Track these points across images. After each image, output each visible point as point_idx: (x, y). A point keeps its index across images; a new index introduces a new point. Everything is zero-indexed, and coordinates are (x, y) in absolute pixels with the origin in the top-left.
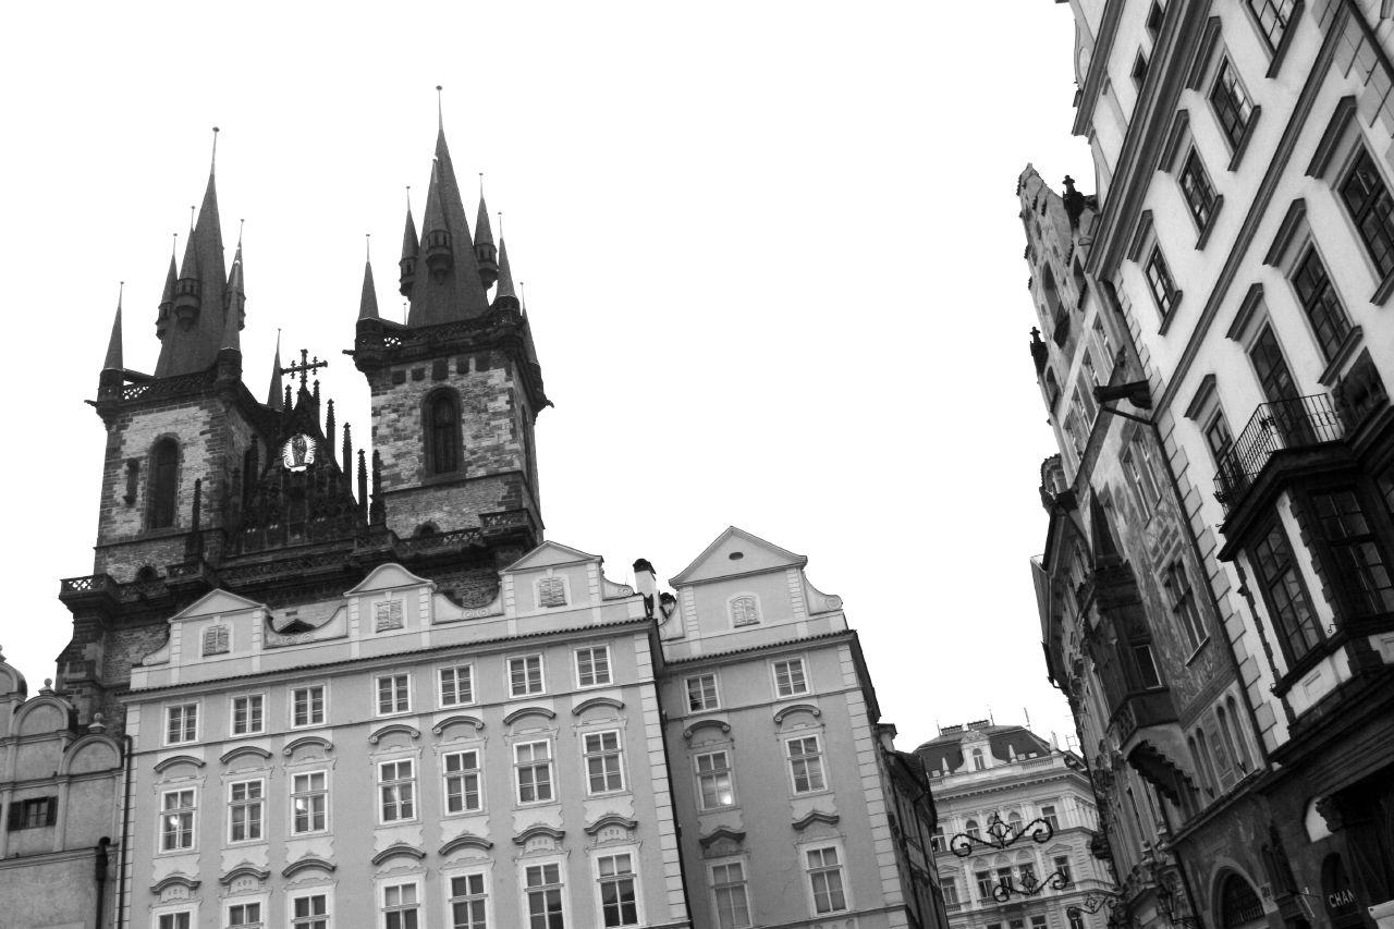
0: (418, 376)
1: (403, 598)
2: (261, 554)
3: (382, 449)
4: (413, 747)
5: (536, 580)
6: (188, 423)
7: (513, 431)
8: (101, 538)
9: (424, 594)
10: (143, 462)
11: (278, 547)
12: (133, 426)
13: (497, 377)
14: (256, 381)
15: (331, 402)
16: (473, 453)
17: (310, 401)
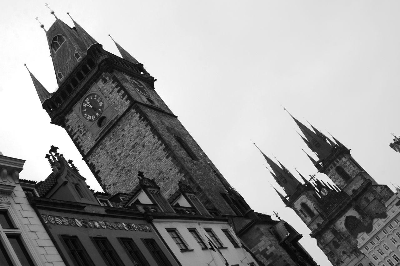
0: (332, 168)
1: (378, 221)
2: (333, 210)
3: (336, 182)
4: (392, 235)
5: (390, 211)
6: (303, 199)
7: (354, 166)
8: (307, 225)
9: (380, 220)
10: (302, 209)
11: (334, 208)
12: (295, 205)
13: (344, 159)
14: (303, 183)
15: (322, 181)
16: (351, 174)
17: (318, 182)
